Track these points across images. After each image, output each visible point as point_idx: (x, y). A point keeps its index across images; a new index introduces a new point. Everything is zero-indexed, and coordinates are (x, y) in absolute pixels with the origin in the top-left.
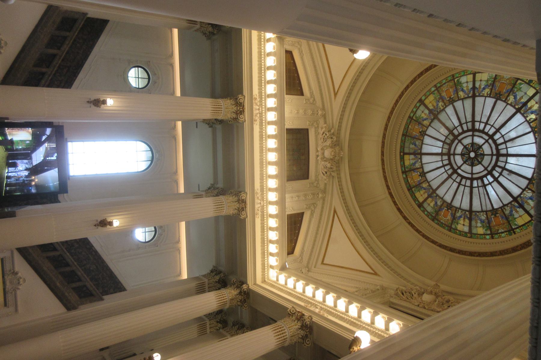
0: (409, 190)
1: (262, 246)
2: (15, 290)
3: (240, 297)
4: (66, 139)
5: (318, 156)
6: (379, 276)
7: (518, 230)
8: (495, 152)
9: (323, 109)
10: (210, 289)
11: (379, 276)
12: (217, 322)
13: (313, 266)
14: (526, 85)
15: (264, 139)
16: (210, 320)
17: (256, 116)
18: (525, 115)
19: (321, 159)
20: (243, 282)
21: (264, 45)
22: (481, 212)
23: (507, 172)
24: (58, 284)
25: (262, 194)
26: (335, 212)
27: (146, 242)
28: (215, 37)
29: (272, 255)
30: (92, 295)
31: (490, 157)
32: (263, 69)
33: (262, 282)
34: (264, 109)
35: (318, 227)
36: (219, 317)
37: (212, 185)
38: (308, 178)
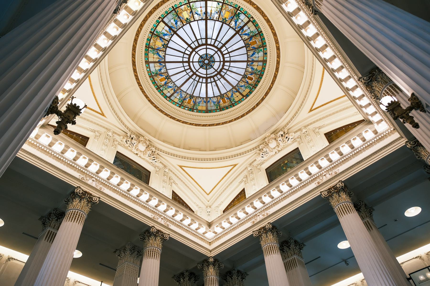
7: (195, 111)
8: (218, 70)
23: (215, 84)
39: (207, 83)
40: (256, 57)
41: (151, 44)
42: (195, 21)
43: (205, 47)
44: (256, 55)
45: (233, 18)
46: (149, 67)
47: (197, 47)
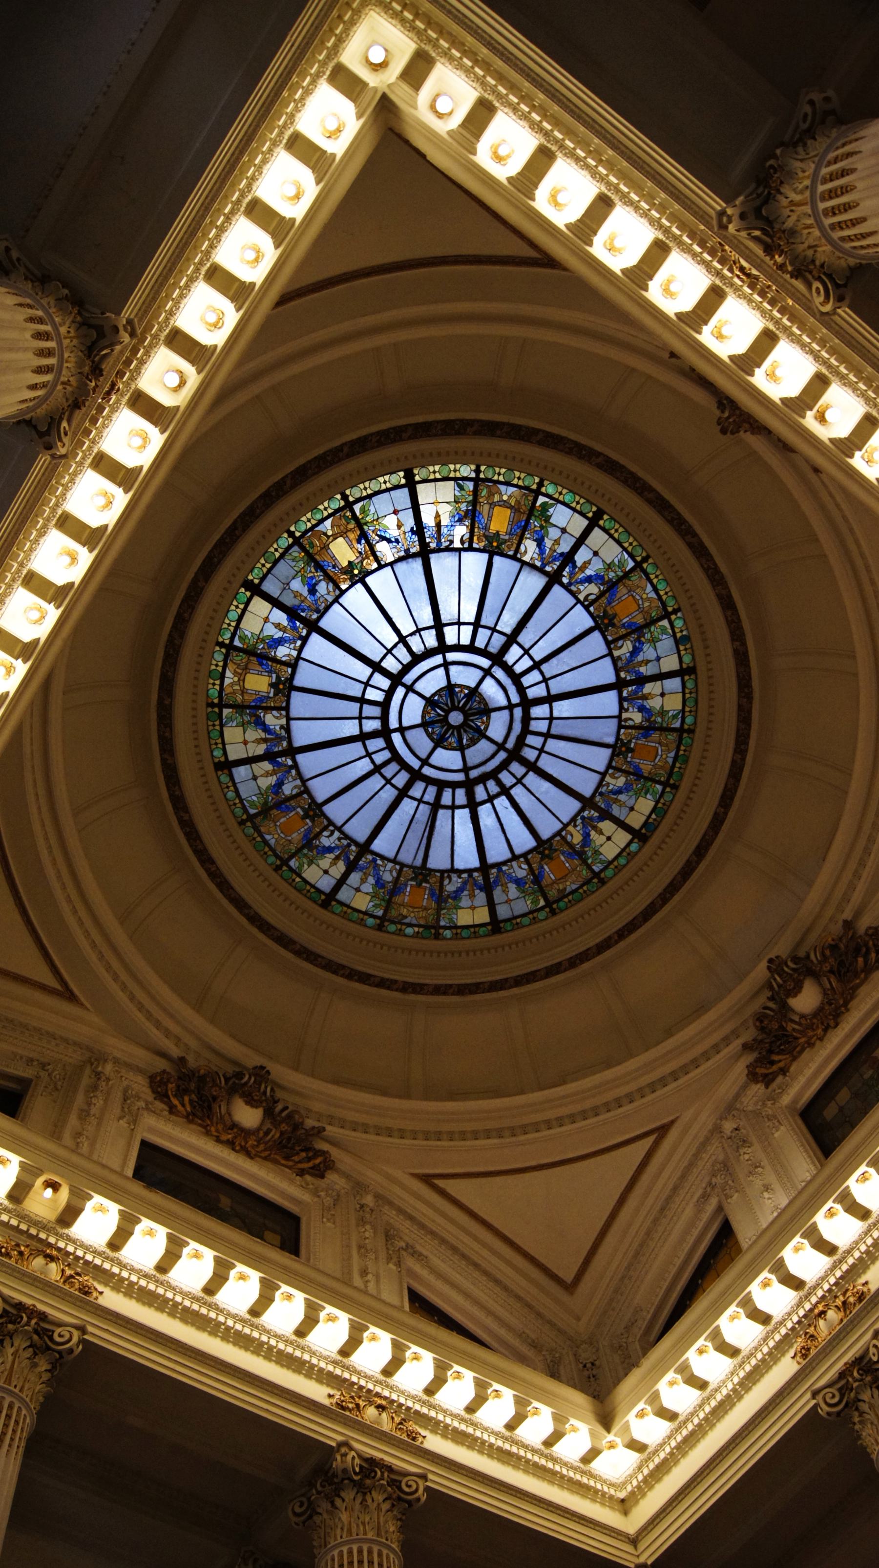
7: (448, 933)
8: (510, 745)
14: (672, 640)
18: (625, 704)
22: (389, 860)
31: (494, 748)
39: (473, 806)
40: (647, 662)
41: (228, 690)
42: (381, 567)
43: (438, 659)
44: (648, 652)
45: (525, 529)
46: (235, 785)
47: (407, 669)
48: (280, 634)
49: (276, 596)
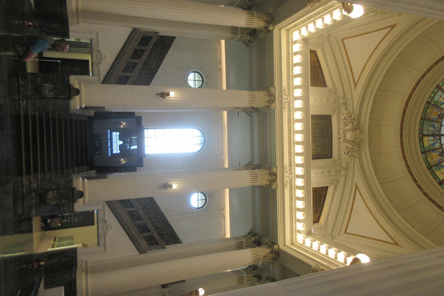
0: (429, 169)
1: (290, 213)
2: (105, 234)
3: (272, 256)
4: (143, 127)
5: (340, 138)
6: (400, 246)
9: (344, 98)
10: (247, 247)
11: (400, 246)
12: (253, 276)
13: (337, 234)
15: (292, 123)
16: (247, 274)
17: (285, 104)
19: (343, 140)
20: (274, 243)
21: (292, 46)
24: (134, 233)
25: (291, 169)
26: (357, 187)
27: (198, 208)
28: (253, 44)
29: (299, 221)
30: (157, 243)
32: (291, 66)
33: (291, 245)
34: (291, 98)
35: (341, 200)
36: (255, 272)
37: (250, 162)
38: (331, 157)
48: (433, 142)
49: (427, 134)
